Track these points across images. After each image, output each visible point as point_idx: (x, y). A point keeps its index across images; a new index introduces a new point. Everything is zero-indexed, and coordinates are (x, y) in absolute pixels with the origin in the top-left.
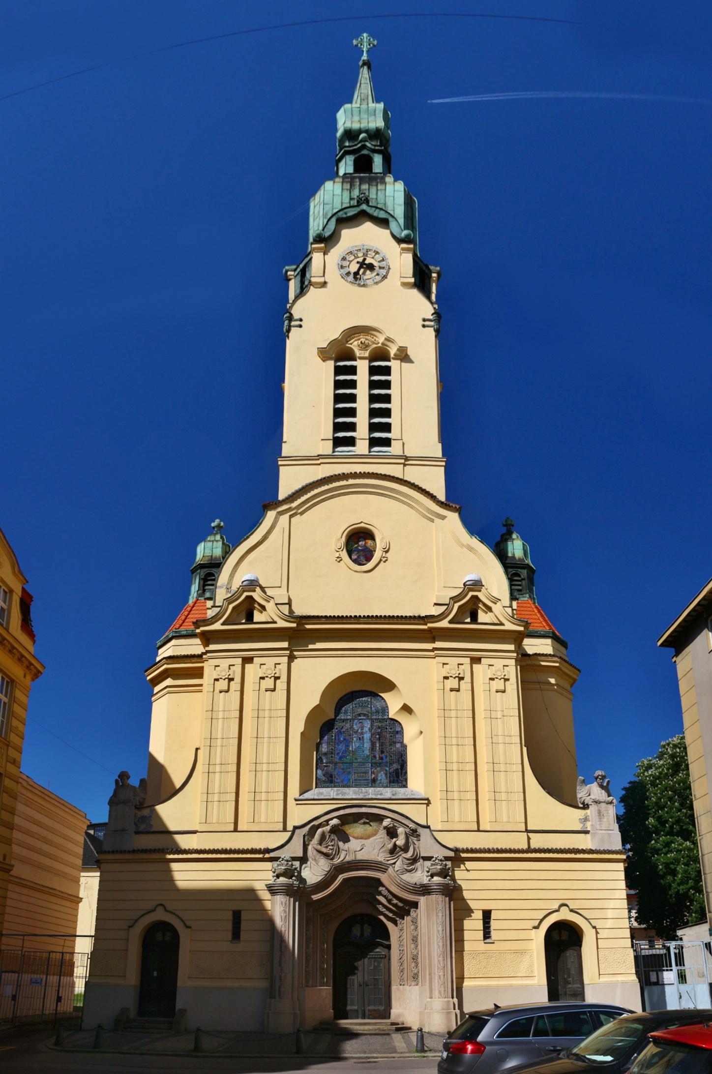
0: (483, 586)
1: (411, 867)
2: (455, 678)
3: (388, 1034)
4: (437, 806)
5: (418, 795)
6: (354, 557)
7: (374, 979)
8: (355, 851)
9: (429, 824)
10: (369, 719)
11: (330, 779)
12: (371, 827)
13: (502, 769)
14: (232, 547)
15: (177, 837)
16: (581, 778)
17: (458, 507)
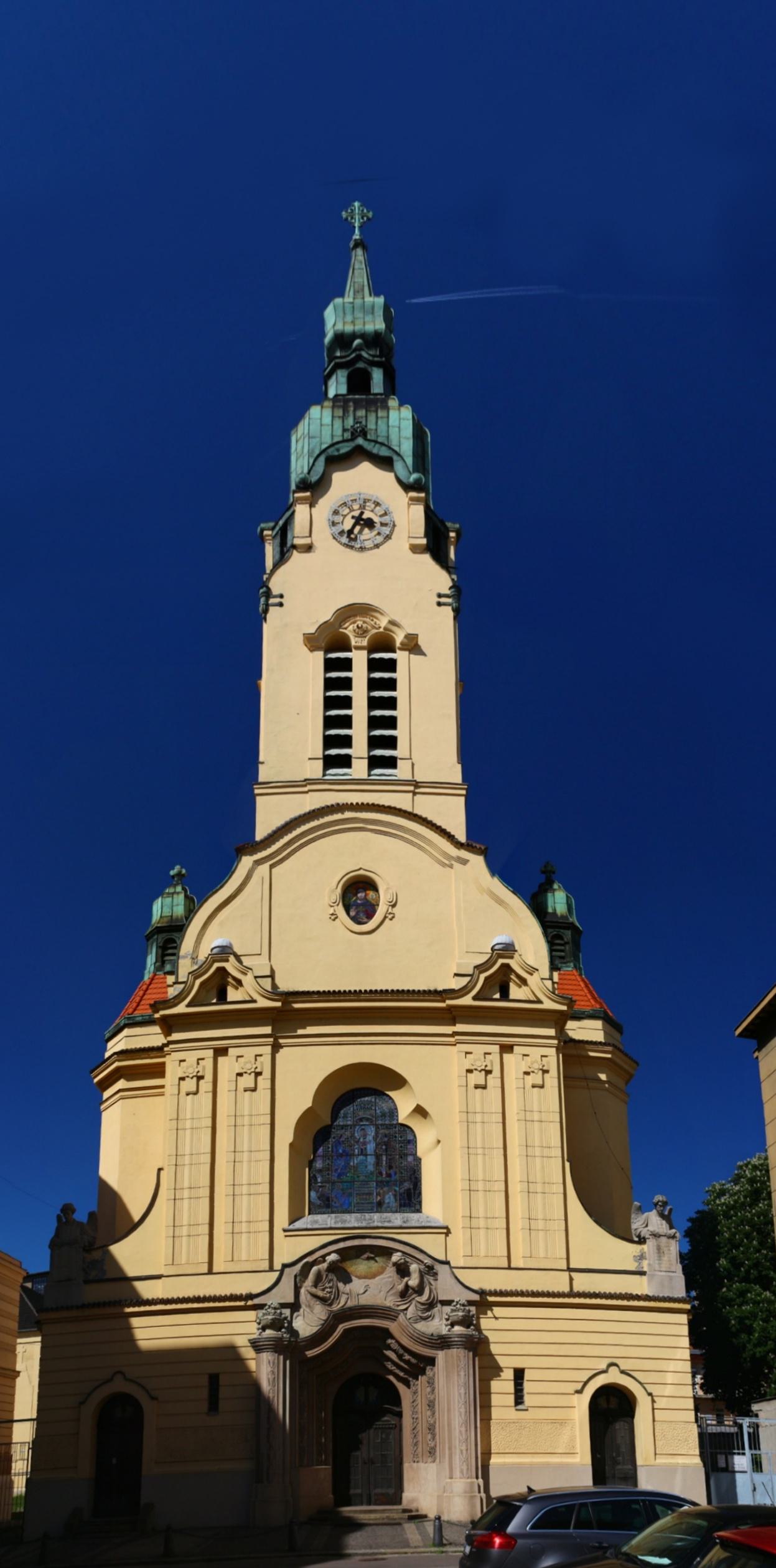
0: (516, 951)
1: (426, 1314)
2: (480, 1071)
3: (399, 1524)
4: (459, 1236)
5: (435, 1223)
6: (352, 913)
7: (382, 1455)
8: (358, 1295)
9: (448, 1259)
10: (373, 1124)
11: (327, 1203)
12: (376, 1264)
13: (539, 1190)
14: (198, 904)
15: (139, 1285)
16: (637, 1203)
17: (483, 848)
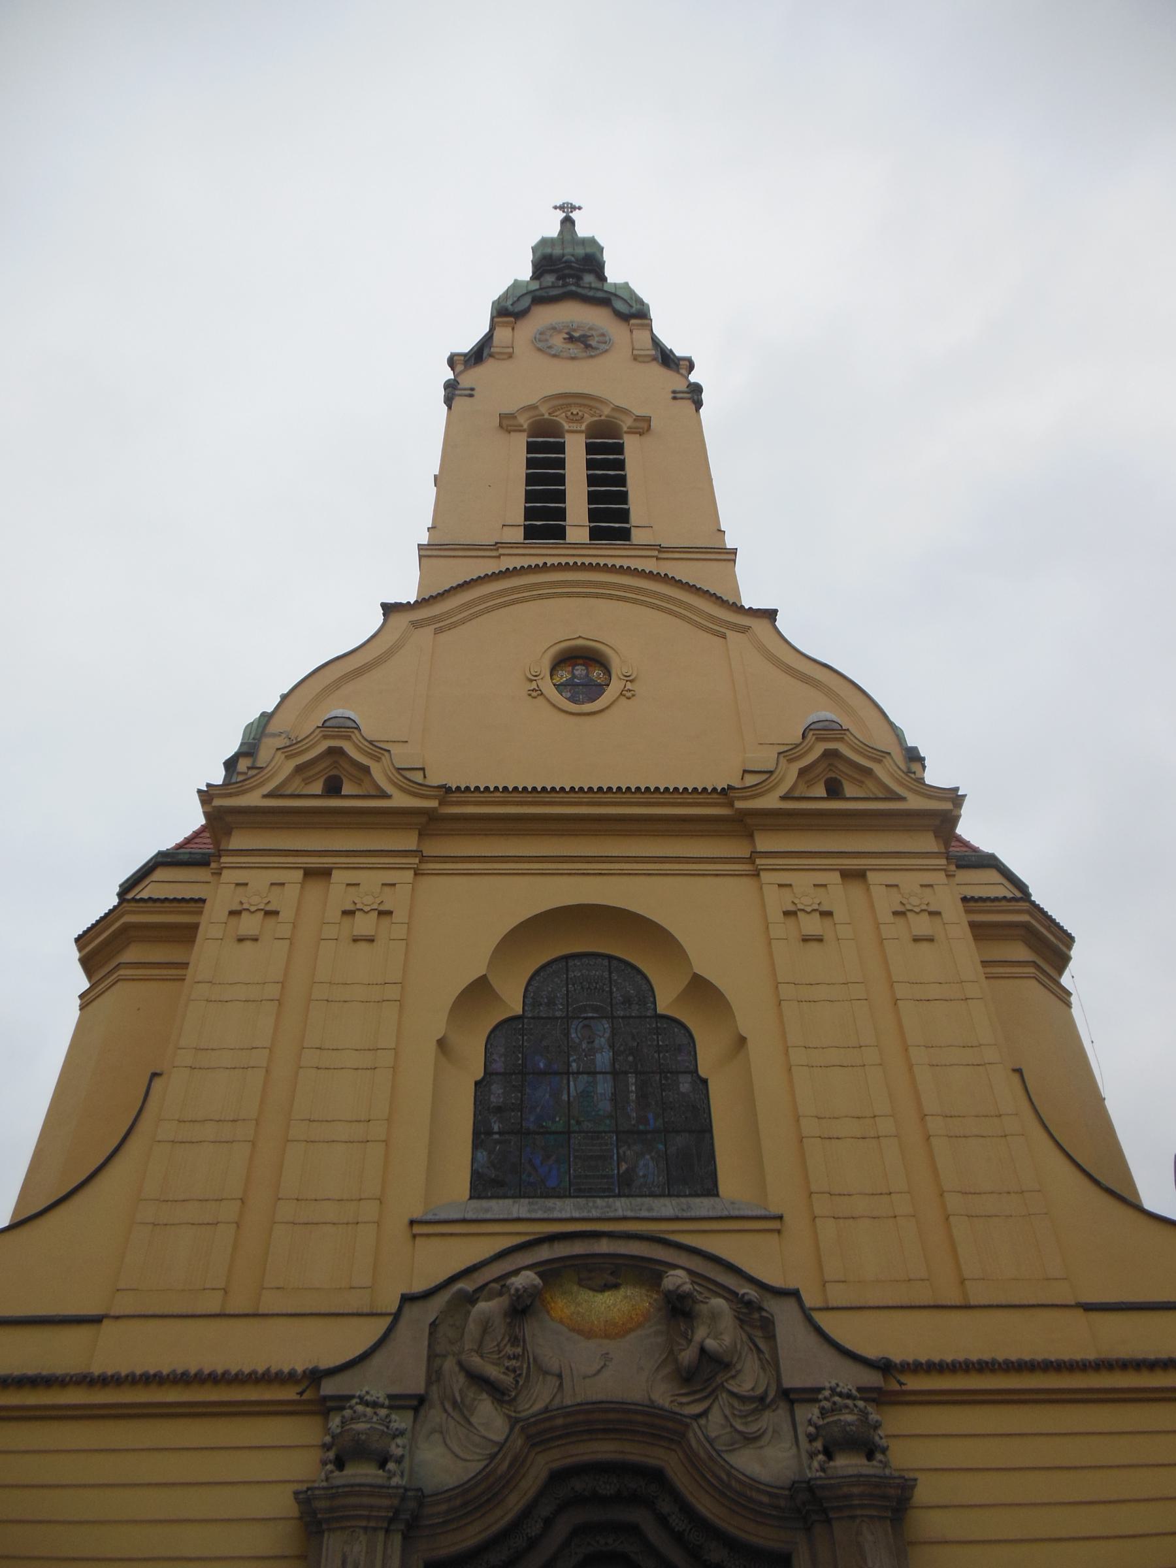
10: (606, 1018)
